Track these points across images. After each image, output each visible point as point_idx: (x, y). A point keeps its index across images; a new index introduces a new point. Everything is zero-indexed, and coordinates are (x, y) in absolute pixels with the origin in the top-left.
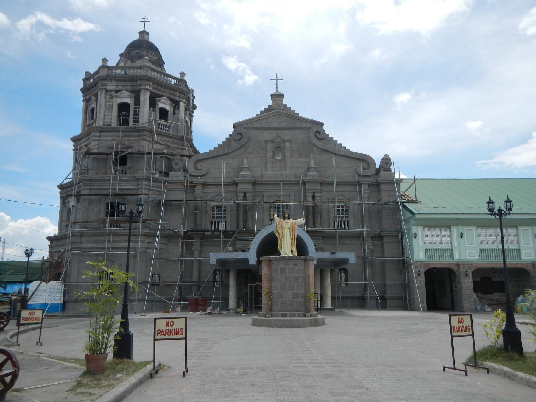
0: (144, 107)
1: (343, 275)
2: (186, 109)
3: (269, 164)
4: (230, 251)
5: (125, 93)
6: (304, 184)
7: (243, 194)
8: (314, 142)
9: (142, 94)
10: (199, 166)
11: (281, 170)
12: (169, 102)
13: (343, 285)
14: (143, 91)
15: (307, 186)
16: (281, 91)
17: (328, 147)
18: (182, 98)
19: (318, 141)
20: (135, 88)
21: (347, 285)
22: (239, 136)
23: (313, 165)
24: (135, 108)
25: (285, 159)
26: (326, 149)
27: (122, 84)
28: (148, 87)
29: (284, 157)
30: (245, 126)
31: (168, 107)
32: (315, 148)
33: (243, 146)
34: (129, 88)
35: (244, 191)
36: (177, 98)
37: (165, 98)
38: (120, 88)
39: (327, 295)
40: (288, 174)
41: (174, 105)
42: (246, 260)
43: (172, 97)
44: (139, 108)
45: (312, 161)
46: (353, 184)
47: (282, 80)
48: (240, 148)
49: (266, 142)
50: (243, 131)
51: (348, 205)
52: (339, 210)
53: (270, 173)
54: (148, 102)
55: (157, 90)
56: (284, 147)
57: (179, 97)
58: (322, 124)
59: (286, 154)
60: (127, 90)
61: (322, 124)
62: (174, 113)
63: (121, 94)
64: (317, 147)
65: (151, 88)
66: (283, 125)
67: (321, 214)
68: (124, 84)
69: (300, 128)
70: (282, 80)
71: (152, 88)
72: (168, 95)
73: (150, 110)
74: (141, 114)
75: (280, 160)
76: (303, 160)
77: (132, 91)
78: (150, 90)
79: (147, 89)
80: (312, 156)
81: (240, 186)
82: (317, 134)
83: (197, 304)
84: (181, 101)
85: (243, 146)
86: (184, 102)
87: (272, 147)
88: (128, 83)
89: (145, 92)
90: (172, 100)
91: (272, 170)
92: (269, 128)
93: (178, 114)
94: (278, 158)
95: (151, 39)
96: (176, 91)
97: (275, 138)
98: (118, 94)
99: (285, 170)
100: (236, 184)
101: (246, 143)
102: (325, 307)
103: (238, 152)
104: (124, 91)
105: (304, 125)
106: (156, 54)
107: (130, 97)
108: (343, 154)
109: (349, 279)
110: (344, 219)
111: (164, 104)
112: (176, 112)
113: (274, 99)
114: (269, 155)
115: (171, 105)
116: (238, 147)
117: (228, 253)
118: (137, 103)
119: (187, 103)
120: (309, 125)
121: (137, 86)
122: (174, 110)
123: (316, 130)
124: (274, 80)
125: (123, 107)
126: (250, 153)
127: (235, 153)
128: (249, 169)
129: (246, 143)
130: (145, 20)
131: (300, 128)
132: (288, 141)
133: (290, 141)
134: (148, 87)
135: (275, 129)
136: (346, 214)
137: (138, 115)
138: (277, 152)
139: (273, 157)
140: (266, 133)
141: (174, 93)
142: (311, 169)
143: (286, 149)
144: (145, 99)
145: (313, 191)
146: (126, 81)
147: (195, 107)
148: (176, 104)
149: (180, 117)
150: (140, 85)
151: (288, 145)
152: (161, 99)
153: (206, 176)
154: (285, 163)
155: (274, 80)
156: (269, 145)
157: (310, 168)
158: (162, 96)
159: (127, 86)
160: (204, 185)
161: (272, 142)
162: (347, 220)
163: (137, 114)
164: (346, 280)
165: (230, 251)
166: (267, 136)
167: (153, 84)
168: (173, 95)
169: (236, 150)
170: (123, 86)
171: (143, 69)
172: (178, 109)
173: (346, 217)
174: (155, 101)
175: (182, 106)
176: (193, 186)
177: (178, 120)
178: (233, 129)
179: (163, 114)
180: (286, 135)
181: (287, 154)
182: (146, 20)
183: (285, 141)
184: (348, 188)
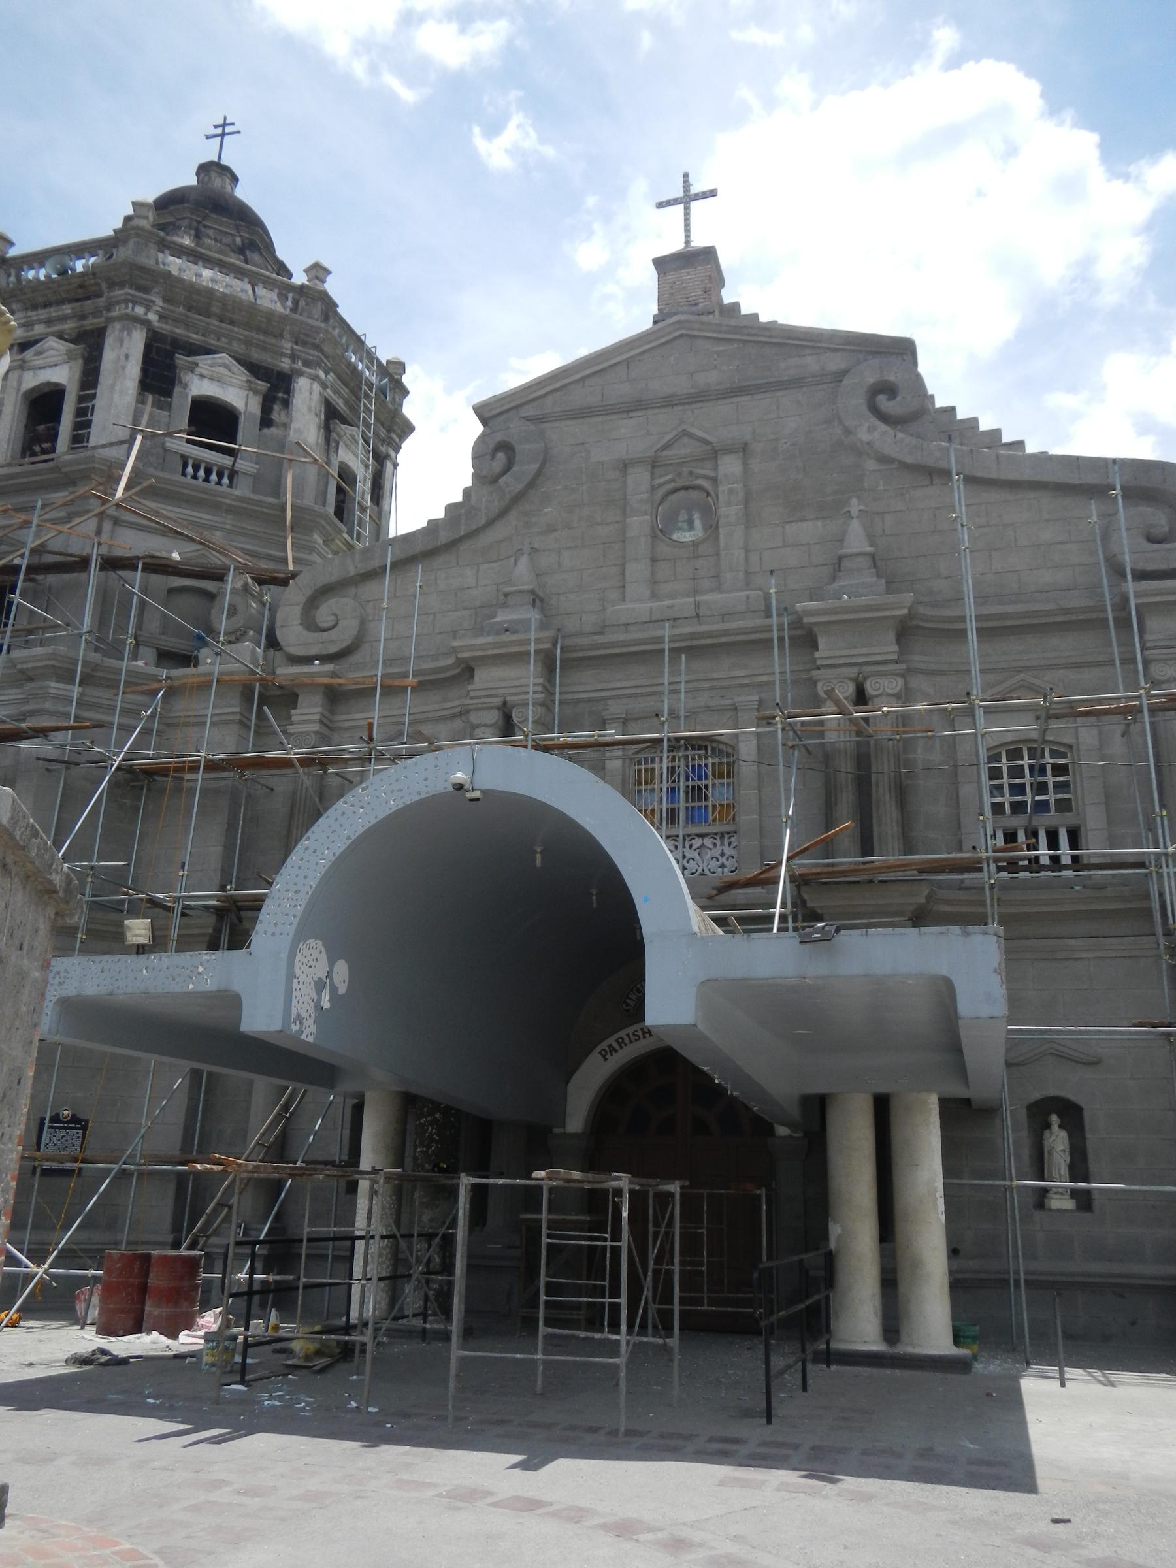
0: (112, 387)
1: (1058, 1140)
2: (332, 416)
3: (638, 570)
4: (140, 949)
5: (55, 347)
6: (805, 639)
7: (494, 717)
8: (863, 435)
9: (109, 342)
10: (324, 615)
11: (696, 592)
12: (241, 375)
13: (1061, 1203)
14: (117, 326)
15: (826, 648)
16: (699, 241)
17: (933, 451)
18: (307, 363)
19: (883, 427)
20: (90, 323)
21: (1084, 1200)
22: (501, 456)
23: (856, 541)
24: (81, 399)
25: (717, 538)
26: (930, 462)
27: (43, 314)
28: (140, 310)
29: (712, 528)
30: (529, 411)
31: (235, 392)
32: (871, 465)
33: (518, 498)
34: (69, 326)
35: (498, 701)
36: (285, 364)
37: (224, 357)
38: (39, 329)
39: (916, 1264)
40: (728, 603)
41: (263, 386)
42: (232, 1002)
43: (256, 356)
44: (94, 396)
45: (855, 525)
46: (1091, 623)
47: (712, 193)
48: (503, 513)
49: (624, 466)
50: (515, 429)
51: (1061, 731)
52: (1016, 772)
53: (637, 605)
54: (134, 369)
55: (187, 326)
56: (715, 480)
57: (293, 357)
58: (904, 349)
59: (723, 510)
60: (60, 336)
61: (904, 349)
62: (266, 421)
63: (39, 353)
64: (884, 459)
65: (153, 317)
66: (711, 379)
67: (902, 793)
68: (53, 312)
69: (796, 383)
70: (712, 193)
71: (162, 317)
72: (235, 346)
73: (141, 400)
74: (97, 419)
75: (695, 544)
76: (810, 530)
77: (78, 338)
78: (146, 323)
79: (136, 320)
80: (855, 506)
81: (484, 678)
82: (881, 399)
83: (143, 1289)
84: (301, 374)
85: (518, 498)
86: (315, 378)
87: (653, 489)
88: (67, 309)
89: (122, 330)
90: (255, 369)
91: (654, 596)
92: (636, 406)
93: (286, 426)
94: (687, 537)
95: (243, 192)
96: (281, 336)
97: (665, 447)
98: (29, 354)
99: (719, 589)
100: (467, 671)
101: (532, 484)
102: (904, 1349)
103: (500, 531)
104: (52, 342)
105: (812, 363)
106: (237, 228)
107: (70, 357)
108: (1028, 475)
109: (1093, 1166)
110: (1052, 818)
111: (217, 380)
112: (277, 414)
113: (671, 277)
114: (639, 524)
115: (251, 388)
116: (496, 506)
117: (130, 960)
118: (90, 378)
119: (345, 391)
120: (835, 363)
121: (96, 313)
122: (266, 410)
123: (871, 380)
124: (676, 202)
125: (43, 406)
126: (551, 529)
127: (486, 539)
128: (537, 599)
129: (532, 484)
130: (223, 130)
131: (796, 383)
132: (729, 450)
133: (744, 450)
134: (140, 310)
135: (670, 402)
136: (1061, 787)
137: (88, 424)
138: (683, 516)
139: (661, 533)
140: (625, 427)
141: (273, 341)
142: (846, 564)
143: (723, 488)
144: (124, 359)
145: (853, 672)
146: (60, 302)
147: (407, 429)
148: (276, 388)
149: (293, 436)
150: (109, 309)
151: (730, 466)
152: (204, 362)
153: (355, 658)
154: (718, 554)
155: (676, 202)
156: (639, 478)
157: (840, 559)
158: (208, 351)
159: (63, 319)
160: (335, 696)
161: (654, 464)
162: (1070, 819)
163: (83, 423)
164: (1079, 1169)
165: (140, 949)
166: (631, 437)
167: (165, 300)
168: (264, 348)
169: (490, 523)
170: (49, 322)
171: (125, 242)
172: (286, 404)
173: (1064, 806)
174: (172, 367)
175: (307, 395)
176: (284, 699)
177: (281, 447)
178: (476, 428)
179: (213, 420)
180: (715, 422)
181: (729, 512)
182: (228, 129)
183: (714, 454)
184: (1065, 646)
